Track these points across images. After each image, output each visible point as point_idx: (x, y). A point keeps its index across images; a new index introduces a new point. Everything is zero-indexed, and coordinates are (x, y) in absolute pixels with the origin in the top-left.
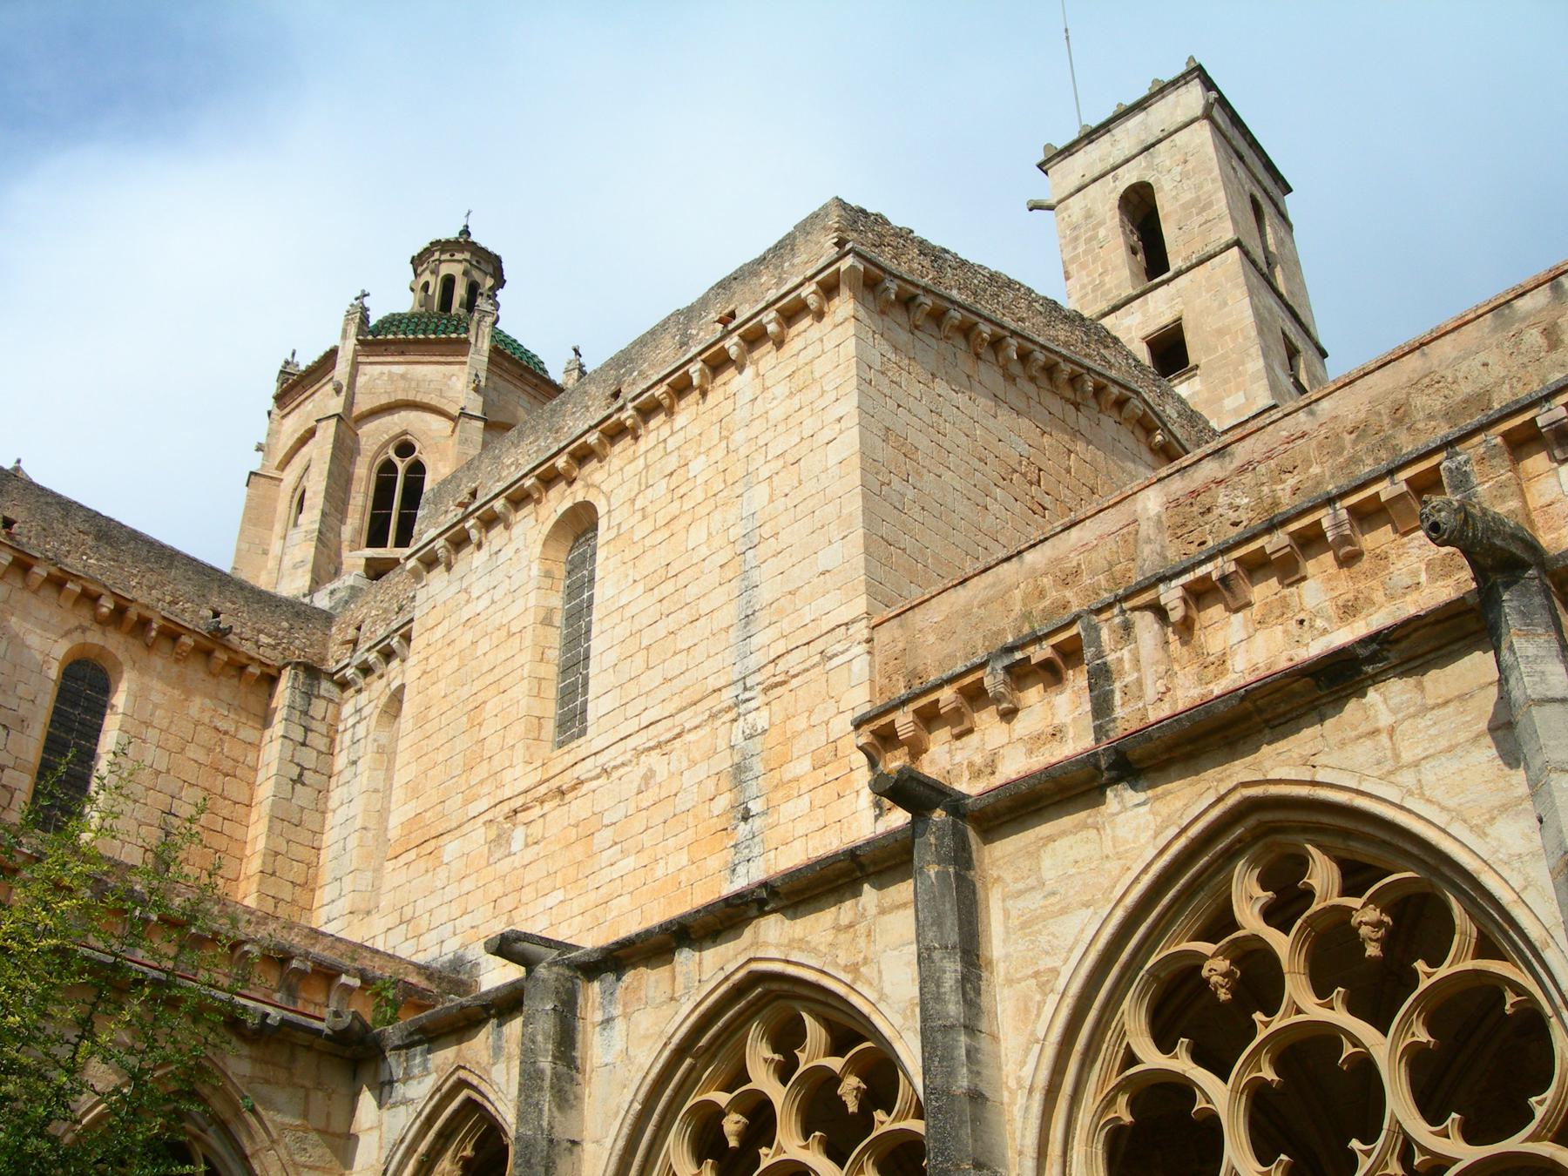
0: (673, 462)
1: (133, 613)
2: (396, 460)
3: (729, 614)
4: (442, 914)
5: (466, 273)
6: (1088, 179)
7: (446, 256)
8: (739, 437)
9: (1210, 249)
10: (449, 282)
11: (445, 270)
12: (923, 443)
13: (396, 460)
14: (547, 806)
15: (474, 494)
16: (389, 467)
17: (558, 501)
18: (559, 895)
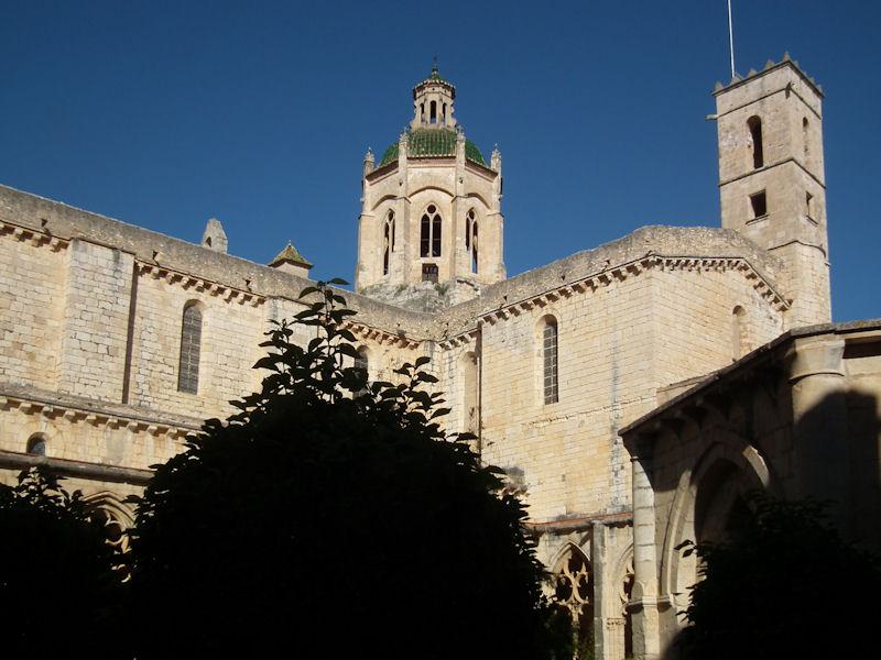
0: (586, 312)
1: (374, 332)
2: (428, 214)
3: (609, 374)
4: (509, 452)
5: (441, 100)
6: (733, 108)
7: (430, 90)
8: (611, 310)
9: (781, 159)
10: (433, 104)
11: (431, 98)
12: (671, 317)
13: (428, 214)
14: (546, 423)
15: (505, 298)
16: (425, 218)
17: (539, 312)
18: (552, 454)
